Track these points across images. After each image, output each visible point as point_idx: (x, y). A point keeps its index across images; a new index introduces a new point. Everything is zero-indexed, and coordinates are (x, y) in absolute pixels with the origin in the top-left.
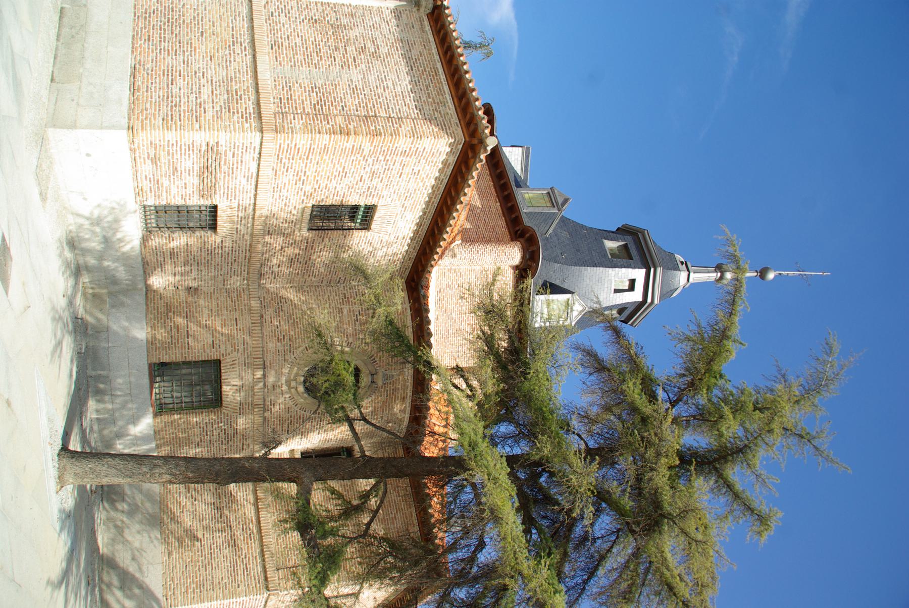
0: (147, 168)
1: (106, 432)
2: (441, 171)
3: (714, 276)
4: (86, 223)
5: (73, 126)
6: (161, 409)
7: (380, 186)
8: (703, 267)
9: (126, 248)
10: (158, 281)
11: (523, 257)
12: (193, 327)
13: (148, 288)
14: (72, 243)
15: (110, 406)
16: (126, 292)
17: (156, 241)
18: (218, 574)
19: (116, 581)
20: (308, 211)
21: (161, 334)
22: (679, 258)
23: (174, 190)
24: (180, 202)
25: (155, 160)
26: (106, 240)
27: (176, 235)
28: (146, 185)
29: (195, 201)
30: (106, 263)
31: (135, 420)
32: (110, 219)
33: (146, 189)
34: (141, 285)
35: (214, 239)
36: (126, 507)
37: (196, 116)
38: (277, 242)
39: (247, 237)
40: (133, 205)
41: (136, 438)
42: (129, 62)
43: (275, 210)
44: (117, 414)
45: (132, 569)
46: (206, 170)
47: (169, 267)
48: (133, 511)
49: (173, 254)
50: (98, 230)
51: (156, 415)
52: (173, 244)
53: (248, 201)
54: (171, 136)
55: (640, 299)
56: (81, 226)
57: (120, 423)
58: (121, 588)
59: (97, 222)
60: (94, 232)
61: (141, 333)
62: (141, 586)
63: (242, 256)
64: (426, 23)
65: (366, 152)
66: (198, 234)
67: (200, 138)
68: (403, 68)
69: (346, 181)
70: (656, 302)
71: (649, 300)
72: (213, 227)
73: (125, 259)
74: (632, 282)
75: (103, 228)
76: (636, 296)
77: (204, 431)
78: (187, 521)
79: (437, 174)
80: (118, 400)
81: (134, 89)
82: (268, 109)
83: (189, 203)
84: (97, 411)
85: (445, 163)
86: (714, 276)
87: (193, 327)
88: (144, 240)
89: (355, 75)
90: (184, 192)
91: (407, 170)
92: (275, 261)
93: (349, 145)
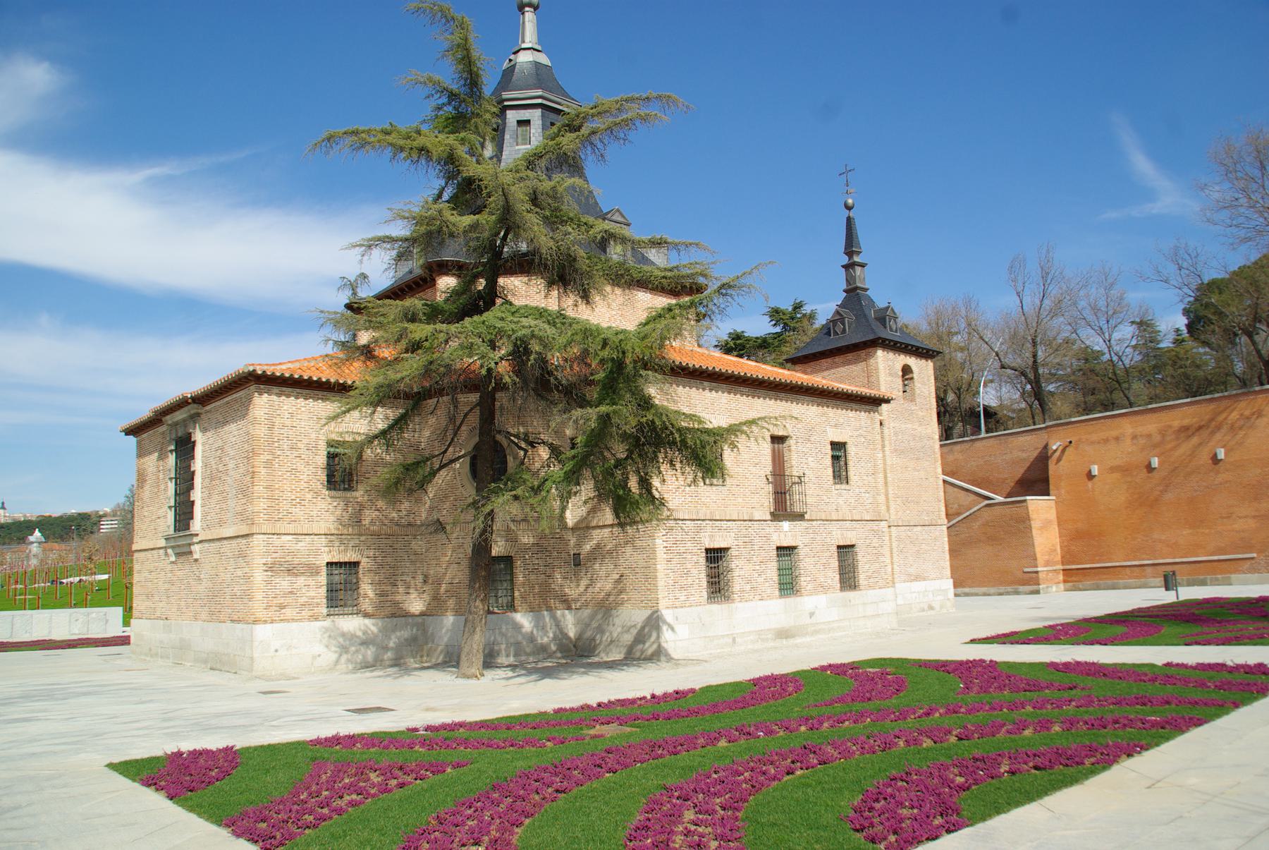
0: (289, 612)
1: (528, 650)
2: (288, 396)
3: (529, 16)
4: (344, 657)
5: (252, 658)
6: (511, 607)
7: (305, 441)
8: (518, 30)
9: (374, 629)
10: (416, 605)
11: (446, 274)
12: (447, 579)
13: (422, 614)
14: (366, 666)
15: (503, 647)
16: (425, 631)
17: (366, 605)
18: (642, 563)
19: (640, 646)
20: (333, 493)
21: (451, 603)
22: (506, 65)
23: (312, 594)
24: (324, 589)
25: (282, 607)
26: (364, 643)
27: (362, 592)
28: (306, 613)
29: (323, 579)
30: (391, 644)
31: (517, 627)
32: (341, 640)
33: (310, 613)
34: (420, 620)
35: (365, 563)
36: (598, 637)
37: (247, 578)
38: (369, 516)
39: (363, 538)
40: (327, 623)
41: (536, 626)
42: (229, 624)
43: (332, 518)
44: (512, 640)
45: (634, 631)
46: (291, 571)
47: (398, 598)
48: (600, 630)
49: (382, 594)
50: (353, 649)
51: (516, 611)
52: (371, 594)
53: (323, 540)
54: (259, 596)
55: (538, 112)
56: (348, 661)
57: (520, 638)
58: (644, 643)
59: (344, 649)
60: (357, 651)
61: (449, 619)
62: (643, 628)
63: (385, 541)
64: (208, 408)
65: (270, 457)
66: (361, 576)
67: (259, 576)
68: (226, 428)
69: (300, 466)
70: (539, 93)
71: (539, 101)
72: (356, 564)
73: (386, 632)
74: (520, 123)
75: (352, 645)
76: (535, 116)
77: (535, 571)
78: (609, 587)
79: (332, 380)
80: (499, 639)
81: (239, 621)
82: (244, 530)
83: (325, 582)
84: (508, 656)
85: (279, 395)
86: (529, 16)
87: (447, 579)
88: (366, 615)
89: (231, 465)
90: (316, 589)
91: (288, 423)
92: (394, 515)
93: (263, 471)
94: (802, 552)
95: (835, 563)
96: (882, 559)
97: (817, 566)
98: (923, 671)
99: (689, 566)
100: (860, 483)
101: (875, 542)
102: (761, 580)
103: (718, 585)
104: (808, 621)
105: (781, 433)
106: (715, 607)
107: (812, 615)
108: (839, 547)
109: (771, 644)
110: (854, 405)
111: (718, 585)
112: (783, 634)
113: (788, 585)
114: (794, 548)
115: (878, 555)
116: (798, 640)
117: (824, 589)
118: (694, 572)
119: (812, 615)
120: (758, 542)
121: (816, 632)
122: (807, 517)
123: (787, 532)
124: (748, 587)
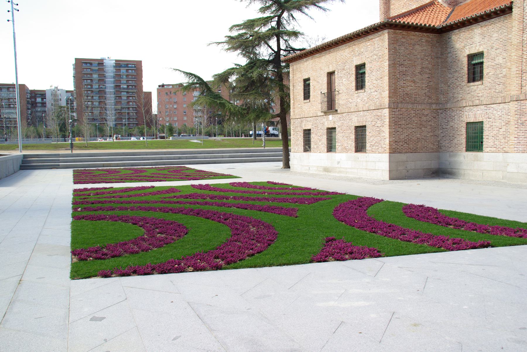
94: (338, 130)
95: (353, 137)
96: (383, 134)
97: (345, 139)
98: (515, 242)
99: (299, 137)
100: (371, 87)
101: (379, 123)
102: (320, 143)
103: (307, 146)
104: (337, 166)
105: (306, 77)
106: (305, 153)
107: (339, 163)
108: (357, 128)
109: (322, 173)
110: (370, 37)
111: (307, 146)
112: (326, 170)
113: (331, 148)
114: (335, 128)
115: (379, 132)
116: (332, 174)
117: (345, 150)
118: (300, 139)
119: (339, 163)
120: (320, 126)
121: (340, 172)
122: (339, 111)
123: (331, 120)
124: (315, 147)
